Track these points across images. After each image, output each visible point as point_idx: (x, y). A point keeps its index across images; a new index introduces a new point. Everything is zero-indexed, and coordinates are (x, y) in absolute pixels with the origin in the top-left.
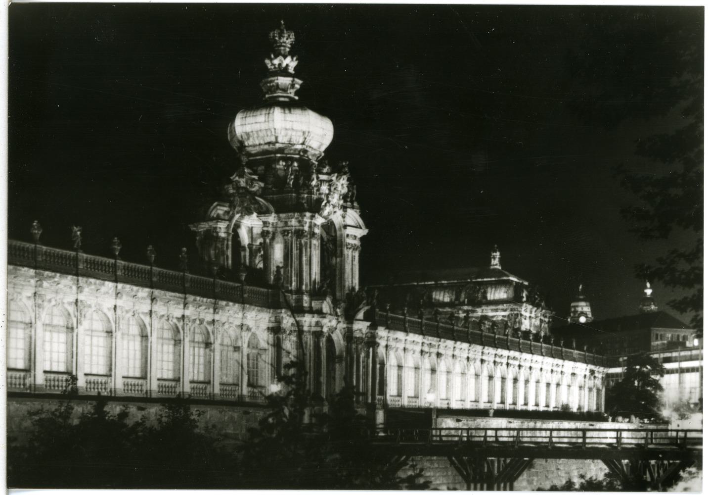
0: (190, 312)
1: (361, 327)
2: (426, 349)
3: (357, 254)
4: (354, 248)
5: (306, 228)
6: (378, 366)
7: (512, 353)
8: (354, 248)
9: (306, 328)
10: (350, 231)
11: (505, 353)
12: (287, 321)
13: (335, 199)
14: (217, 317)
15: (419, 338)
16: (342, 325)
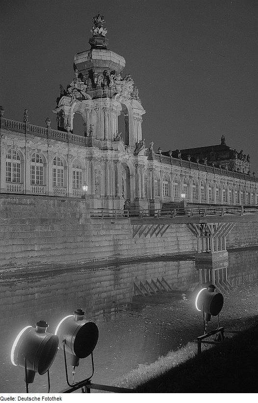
0: (30, 144)
1: (143, 158)
2: (184, 174)
3: (140, 124)
4: (138, 120)
5: (108, 106)
6: (156, 181)
7: (229, 178)
8: (138, 120)
9: (109, 159)
10: (135, 111)
11: (226, 178)
12: (97, 153)
13: (126, 94)
14: (50, 149)
15: (179, 168)
16: (133, 158)
